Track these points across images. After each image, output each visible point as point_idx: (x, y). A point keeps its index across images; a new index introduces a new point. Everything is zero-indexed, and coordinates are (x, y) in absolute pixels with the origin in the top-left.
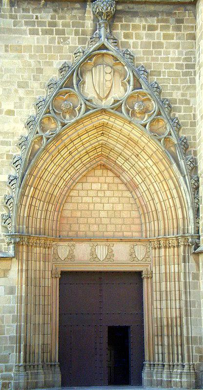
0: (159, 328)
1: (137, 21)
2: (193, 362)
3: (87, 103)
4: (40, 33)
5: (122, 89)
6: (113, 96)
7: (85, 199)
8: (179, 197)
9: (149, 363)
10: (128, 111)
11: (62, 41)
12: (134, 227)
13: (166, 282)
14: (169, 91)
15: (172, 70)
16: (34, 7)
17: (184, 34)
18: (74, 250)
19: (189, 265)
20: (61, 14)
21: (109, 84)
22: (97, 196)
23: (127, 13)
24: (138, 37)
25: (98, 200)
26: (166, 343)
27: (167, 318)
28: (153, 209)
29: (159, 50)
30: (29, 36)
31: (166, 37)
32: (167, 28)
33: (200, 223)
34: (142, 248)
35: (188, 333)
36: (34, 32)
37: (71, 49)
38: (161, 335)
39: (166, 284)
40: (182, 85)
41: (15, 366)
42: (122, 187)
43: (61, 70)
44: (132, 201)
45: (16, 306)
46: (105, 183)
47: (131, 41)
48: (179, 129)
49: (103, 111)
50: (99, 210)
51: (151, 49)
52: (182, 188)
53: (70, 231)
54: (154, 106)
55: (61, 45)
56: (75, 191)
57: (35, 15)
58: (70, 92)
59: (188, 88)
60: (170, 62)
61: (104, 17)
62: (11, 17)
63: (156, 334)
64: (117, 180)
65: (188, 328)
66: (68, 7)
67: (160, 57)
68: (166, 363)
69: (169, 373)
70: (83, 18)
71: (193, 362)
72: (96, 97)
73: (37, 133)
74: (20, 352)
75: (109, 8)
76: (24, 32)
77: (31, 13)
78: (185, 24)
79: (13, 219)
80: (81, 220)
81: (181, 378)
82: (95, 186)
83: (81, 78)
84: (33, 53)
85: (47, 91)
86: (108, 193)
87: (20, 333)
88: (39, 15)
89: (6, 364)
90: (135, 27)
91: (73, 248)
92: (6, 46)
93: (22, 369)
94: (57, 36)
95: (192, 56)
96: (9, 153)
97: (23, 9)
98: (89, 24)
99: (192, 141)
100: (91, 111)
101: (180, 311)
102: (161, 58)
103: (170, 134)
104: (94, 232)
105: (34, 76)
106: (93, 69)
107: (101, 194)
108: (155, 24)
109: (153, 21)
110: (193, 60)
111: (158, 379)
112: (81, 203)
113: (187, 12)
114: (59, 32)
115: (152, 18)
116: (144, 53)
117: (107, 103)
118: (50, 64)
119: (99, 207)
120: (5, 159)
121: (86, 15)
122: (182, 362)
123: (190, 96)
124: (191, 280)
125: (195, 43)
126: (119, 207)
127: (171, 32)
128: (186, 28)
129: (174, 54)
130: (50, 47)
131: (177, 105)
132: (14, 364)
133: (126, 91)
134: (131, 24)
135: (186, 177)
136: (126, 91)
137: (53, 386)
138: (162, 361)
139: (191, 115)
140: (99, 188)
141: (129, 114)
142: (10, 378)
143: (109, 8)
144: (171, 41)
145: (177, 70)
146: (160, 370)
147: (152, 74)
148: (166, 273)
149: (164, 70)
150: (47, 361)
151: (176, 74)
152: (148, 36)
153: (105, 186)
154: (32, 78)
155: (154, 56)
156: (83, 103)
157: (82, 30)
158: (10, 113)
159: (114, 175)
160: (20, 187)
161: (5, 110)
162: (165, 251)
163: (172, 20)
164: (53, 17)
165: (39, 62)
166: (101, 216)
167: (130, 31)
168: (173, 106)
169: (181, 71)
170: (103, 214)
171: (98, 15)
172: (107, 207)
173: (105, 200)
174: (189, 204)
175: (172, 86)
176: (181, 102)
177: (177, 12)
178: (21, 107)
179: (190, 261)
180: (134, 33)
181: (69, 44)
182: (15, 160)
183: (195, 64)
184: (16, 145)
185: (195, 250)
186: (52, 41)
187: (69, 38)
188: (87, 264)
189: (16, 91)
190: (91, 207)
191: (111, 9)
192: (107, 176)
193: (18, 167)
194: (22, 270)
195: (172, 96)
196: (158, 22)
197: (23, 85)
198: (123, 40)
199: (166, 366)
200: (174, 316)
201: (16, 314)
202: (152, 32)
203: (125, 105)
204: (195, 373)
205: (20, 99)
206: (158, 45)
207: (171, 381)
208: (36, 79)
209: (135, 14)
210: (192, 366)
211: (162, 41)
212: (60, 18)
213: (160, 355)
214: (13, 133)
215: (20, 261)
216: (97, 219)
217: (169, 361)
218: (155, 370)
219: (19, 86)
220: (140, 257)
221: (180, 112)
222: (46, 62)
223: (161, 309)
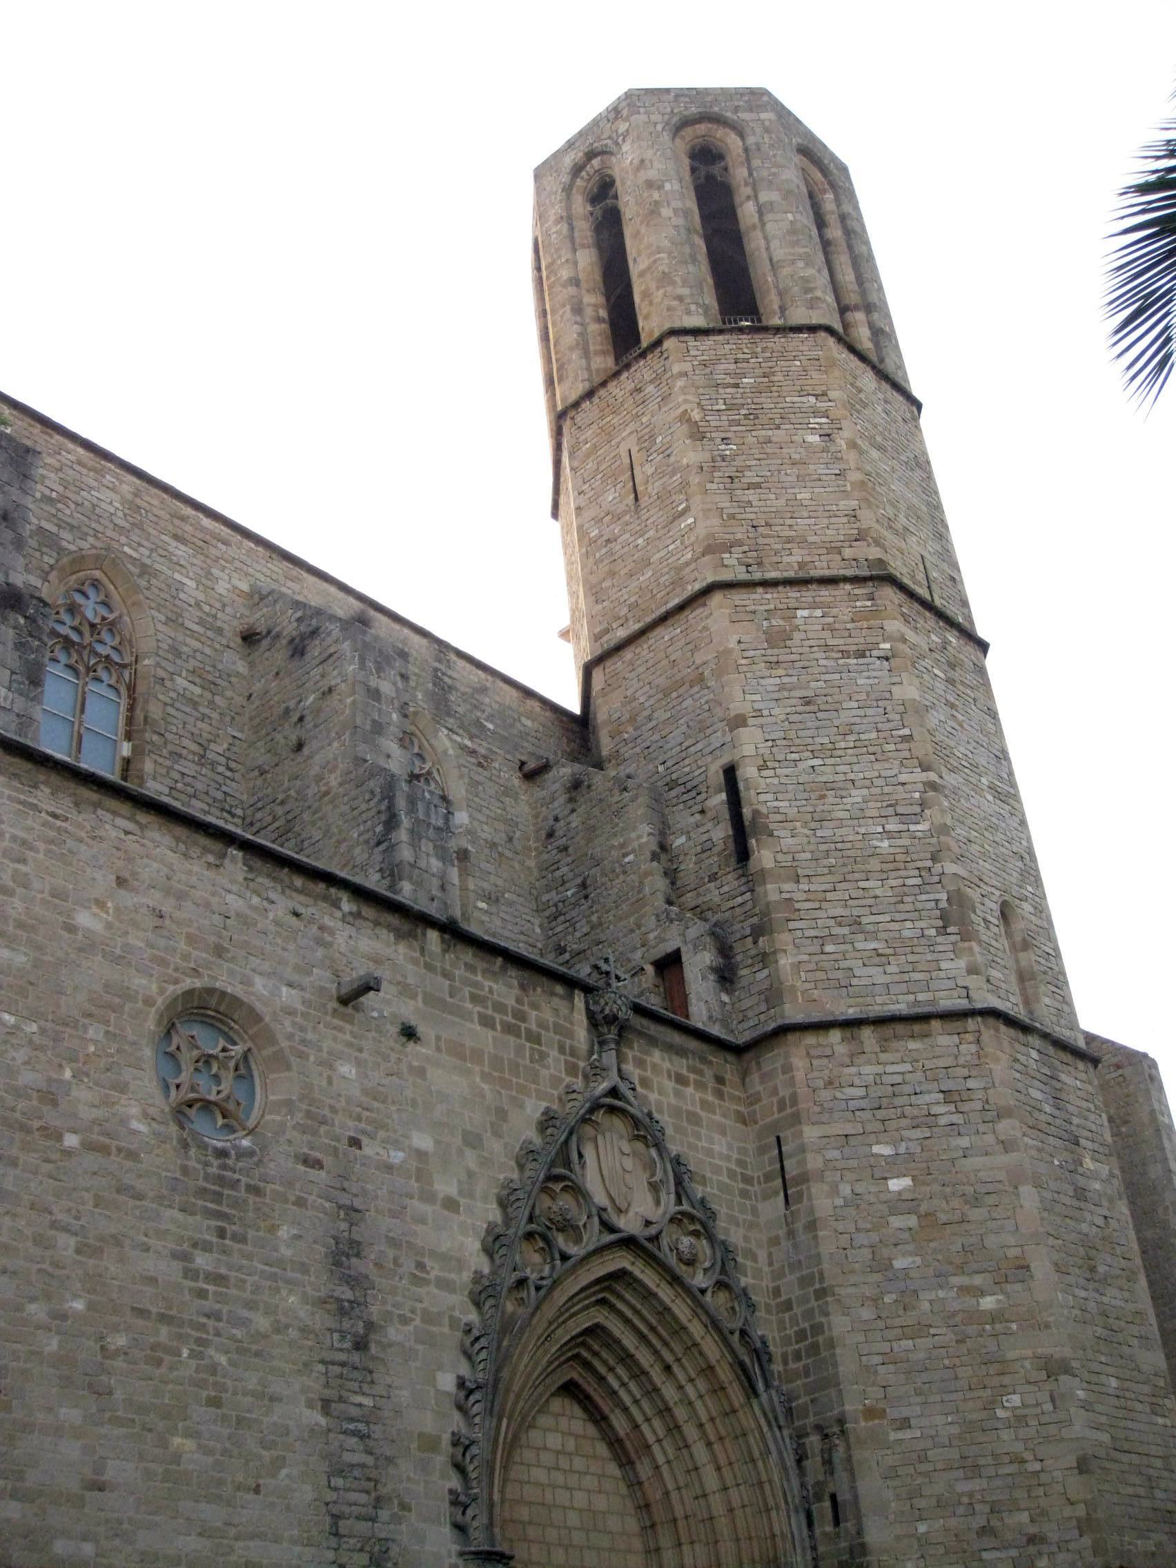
1: (657, 1056)
5: (649, 1198)
7: (539, 1474)
25: (559, 1478)
36: (487, 1022)
42: (602, 1449)
47: (653, 1097)
49: (629, 1243)
62: (445, 975)
64: (591, 1430)
80: (532, 1532)
82: (554, 1441)
86: (579, 1463)
88: (495, 987)
97: (466, 964)
98: (582, 1034)
105: (492, 1124)
106: (600, 1138)
107: (564, 1463)
108: (684, 1072)
109: (681, 1065)
112: (529, 1482)
117: (629, 1224)
119: (563, 1497)
120: (446, 1330)
126: (601, 1503)
127: (710, 1098)
128: (733, 1098)
129: (720, 1146)
133: (658, 1202)
134: (649, 1059)
152: (677, 1094)
156: (594, 1211)
158: (451, 1204)
161: (441, 1196)
163: (709, 1074)
165: (500, 1093)
166: (569, 1524)
170: (573, 1519)
171: (594, 1021)
172: (580, 1499)
181: (548, 1068)
186: (519, 1050)
189: (460, 1152)
197: (472, 1140)
205: (470, 1174)
206: (694, 1119)
208: (497, 1134)
209: (653, 1041)
212: (535, 1006)
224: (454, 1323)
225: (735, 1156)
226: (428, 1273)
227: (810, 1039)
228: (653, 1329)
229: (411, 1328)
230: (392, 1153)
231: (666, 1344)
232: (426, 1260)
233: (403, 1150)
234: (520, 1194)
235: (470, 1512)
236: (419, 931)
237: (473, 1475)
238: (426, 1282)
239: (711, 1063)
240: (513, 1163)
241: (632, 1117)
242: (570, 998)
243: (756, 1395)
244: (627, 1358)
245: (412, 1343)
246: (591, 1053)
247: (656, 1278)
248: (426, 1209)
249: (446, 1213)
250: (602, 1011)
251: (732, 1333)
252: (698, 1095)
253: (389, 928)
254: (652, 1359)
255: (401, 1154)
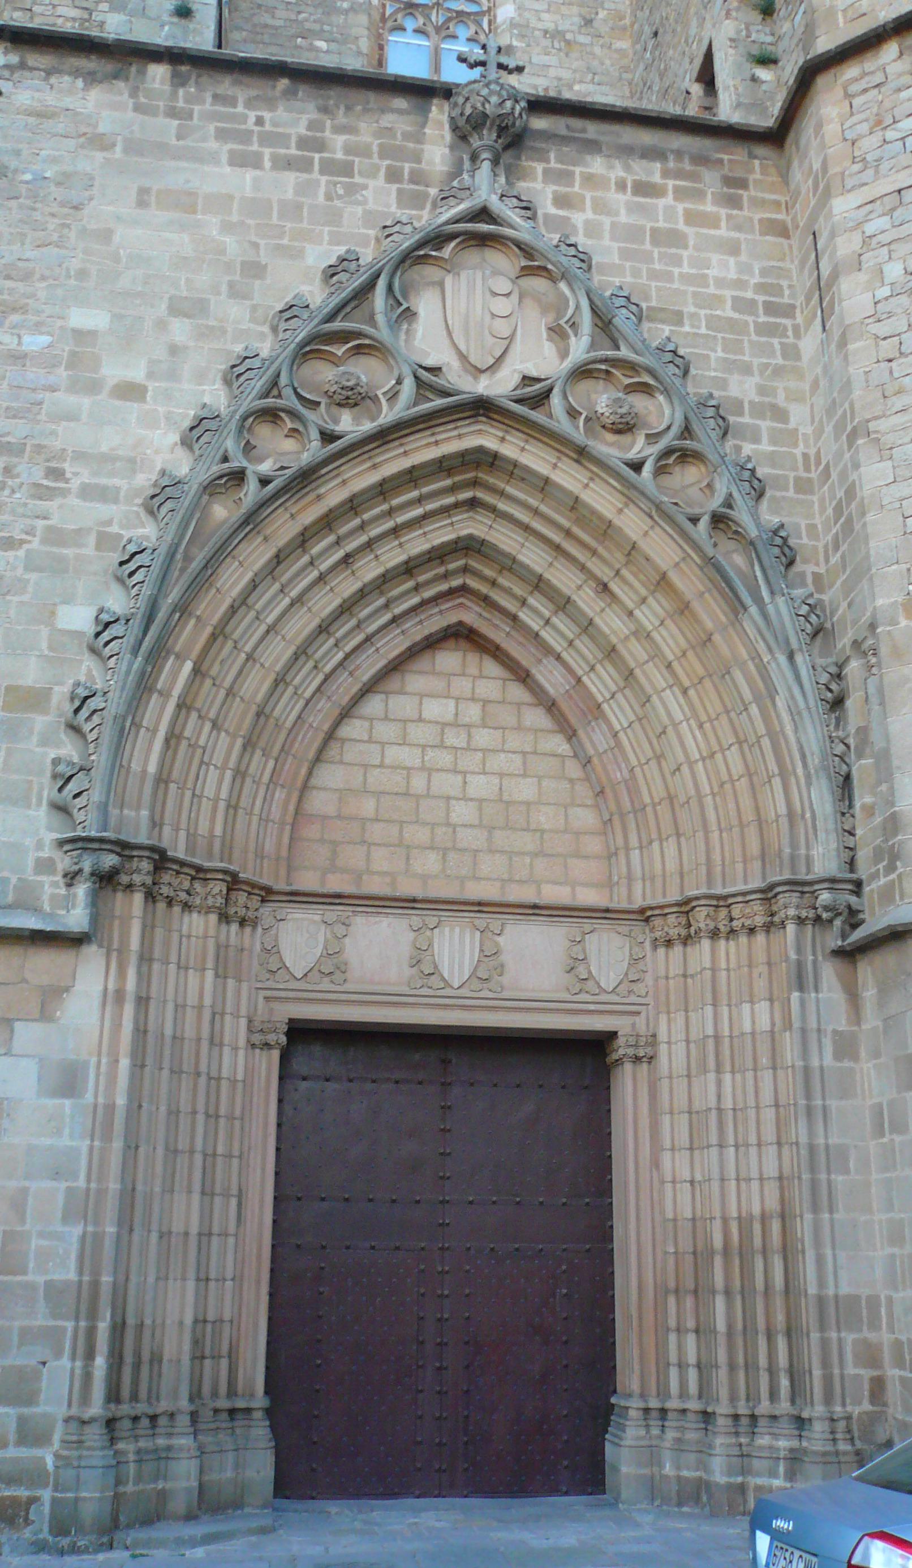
0: (689, 1259)
1: (597, 165)
2: (844, 1405)
3: (422, 373)
4: (267, 164)
5: (549, 349)
6: (519, 367)
7: (395, 754)
8: (771, 734)
9: (642, 1405)
10: (573, 413)
11: (341, 192)
12: (578, 868)
13: (719, 1070)
14: (713, 374)
15: (718, 312)
16: (253, 93)
17: (751, 219)
18: (347, 940)
19: (818, 1000)
20: (341, 118)
21: (503, 328)
22: (441, 746)
23: (565, 140)
24: (600, 207)
25: (445, 759)
26: (721, 1326)
27: (725, 1221)
28: (659, 792)
29: (673, 251)
30: (228, 169)
31: (691, 218)
32: (699, 195)
33: (859, 832)
34: (617, 941)
35: (821, 1283)
36: (241, 161)
37: (369, 218)
38: (696, 1292)
39: (719, 1083)
40: (756, 362)
41: (67, 1420)
42: (537, 718)
43: (331, 273)
44: (574, 769)
45: (85, 1151)
46: (473, 699)
47: (578, 219)
48: (761, 495)
50: (448, 798)
51: (648, 246)
52: (780, 702)
53: (333, 868)
54: (667, 412)
55: (338, 203)
56: (357, 722)
57: (252, 116)
58: (359, 335)
59: (778, 372)
60: (712, 290)
61: (489, 136)
62: (172, 113)
63: (672, 1284)
64: (517, 692)
65: (820, 1261)
66: (368, 103)
67: (676, 271)
68: (722, 1409)
69: (736, 1451)
70: (419, 138)
71: (844, 1405)
72: (456, 364)
73: (225, 459)
74: (90, 1355)
75: (509, 104)
76: (213, 158)
77: (240, 109)
78: (753, 193)
79: (98, 774)
80: (376, 833)
81: (791, 1475)
82: (436, 709)
83: (401, 300)
84: (235, 218)
85: (274, 329)
86: (483, 738)
87: (96, 1273)
88: (267, 115)
89: (26, 1411)
90: (589, 180)
91: (340, 930)
92: (143, 191)
93: (95, 1434)
94: (324, 179)
95: (785, 283)
96: (108, 529)
97: (215, 97)
99: (805, 540)
100: (439, 402)
101: (782, 1188)
102: (680, 274)
103: (728, 503)
104: (425, 878)
105: (231, 285)
106: (449, 280)
107: (455, 738)
108: (657, 178)
109: (653, 172)
110: (787, 292)
111: (685, 1473)
113: (757, 162)
114: (329, 168)
115: (644, 162)
116: (626, 254)
118: (299, 254)
119: (447, 784)
120: (89, 550)
121: (427, 131)
122: (793, 1402)
123: (787, 398)
124: (828, 1060)
125: (791, 247)
126: (525, 790)
127: (708, 207)
128: (758, 203)
130: (299, 207)
131: (746, 419)
132: (61, 1411)
133: (564, 354)
134: (578, 170)
135: (799, 658)
136: (564, 354)
137: (237, 1504)
138: (700, 1397)
139: (793, 456)
140: (449, 717)
141: (577, 428)
142: (35, 1476)
143: (509, 104)
144: (712, 232)
145: (736, 316)
146: (691, 1436)
147: (656, 315)
148: (717, 1038)
149: (692, 309)
150: (215, 1394)
151: (732, 325)
152: (631, 208)
153: (473, 712)
154: (224, 288)
155: (657, 266)
156: (407, 371)
157: (412, 172)
159: (506, 674)
160: (135, 651)
161: (111, 382)
162: (713, 951)
164: (311, 126)
165: (256, 246)
166: (454, 818)
167: (576, 188)
168: (732, 419)
169: (750, 319)
170: (462, 812)
172: (480, 786)
173: (471, 761)
174: (814, 761)
175: (725, 360)
176: (759, 410)
177: (726, 157)
178: (173, 375)
179: (824, 985)
180: (588, 195)
182: (132, 548)
183: (793, 307)
184: (139, 501)
185: (844, 936)
186: (305, 189)
187: (365, 187)
188: (394, 1000)
189: (161, 325)
190: (418, 783)
191: (513, 109)
192: (481, 677)
193: (138, 577)
194: (120, 996)
195: (725, 390)
196: (666, 174)
198: (553, 210)
199: (721, 1421)
200: (756, 1210)
201: (82, 1183)
202: (648, 200)
203: (565, 396)
204: (858, 1453)
205: (174, 350)
206: (672, 238)
207: (742, 1488)
208: (236, 292)
209: (593, 146)
210: (841, 1425)
211: (681, 226)
212: (338, 130)
213: (692, 1374)
214: (132, 461)
215: (115, 954)
216: (440, 831)
217: (733, 1398)
218: (670, 1435)
219: (176, 309)
220: (609, 979)
221: (757, 440)
222: (278, 247)
223: (692, 1182)
224: (104, 540)
225: (756, 279)
226: (67, 481)
227: (851, 71)
228: (568, 533)
229: (21, 553)
230: (26, 339)
231: (594, 553)
232: (66, 466)
233: (49, 334)
234: (256, 363)
235: (72, 787)
236: (133, 69)
237: (91, 737)
238: (64, 493)
239: (721, 161)
240: (266, 329)
241: (518, 244)
242: (425, 112)
243: (746, 609)
244: (539, 584)
245: (19, 571)
246: (457, 172)
247: (551, 457)
248: (86, 402)
249: (118, 403)
250: (462, 114)
251: (694, 520)
252: (680, 207)
253: (76, 73)
254: (578, 578)
255: (44, 340)
